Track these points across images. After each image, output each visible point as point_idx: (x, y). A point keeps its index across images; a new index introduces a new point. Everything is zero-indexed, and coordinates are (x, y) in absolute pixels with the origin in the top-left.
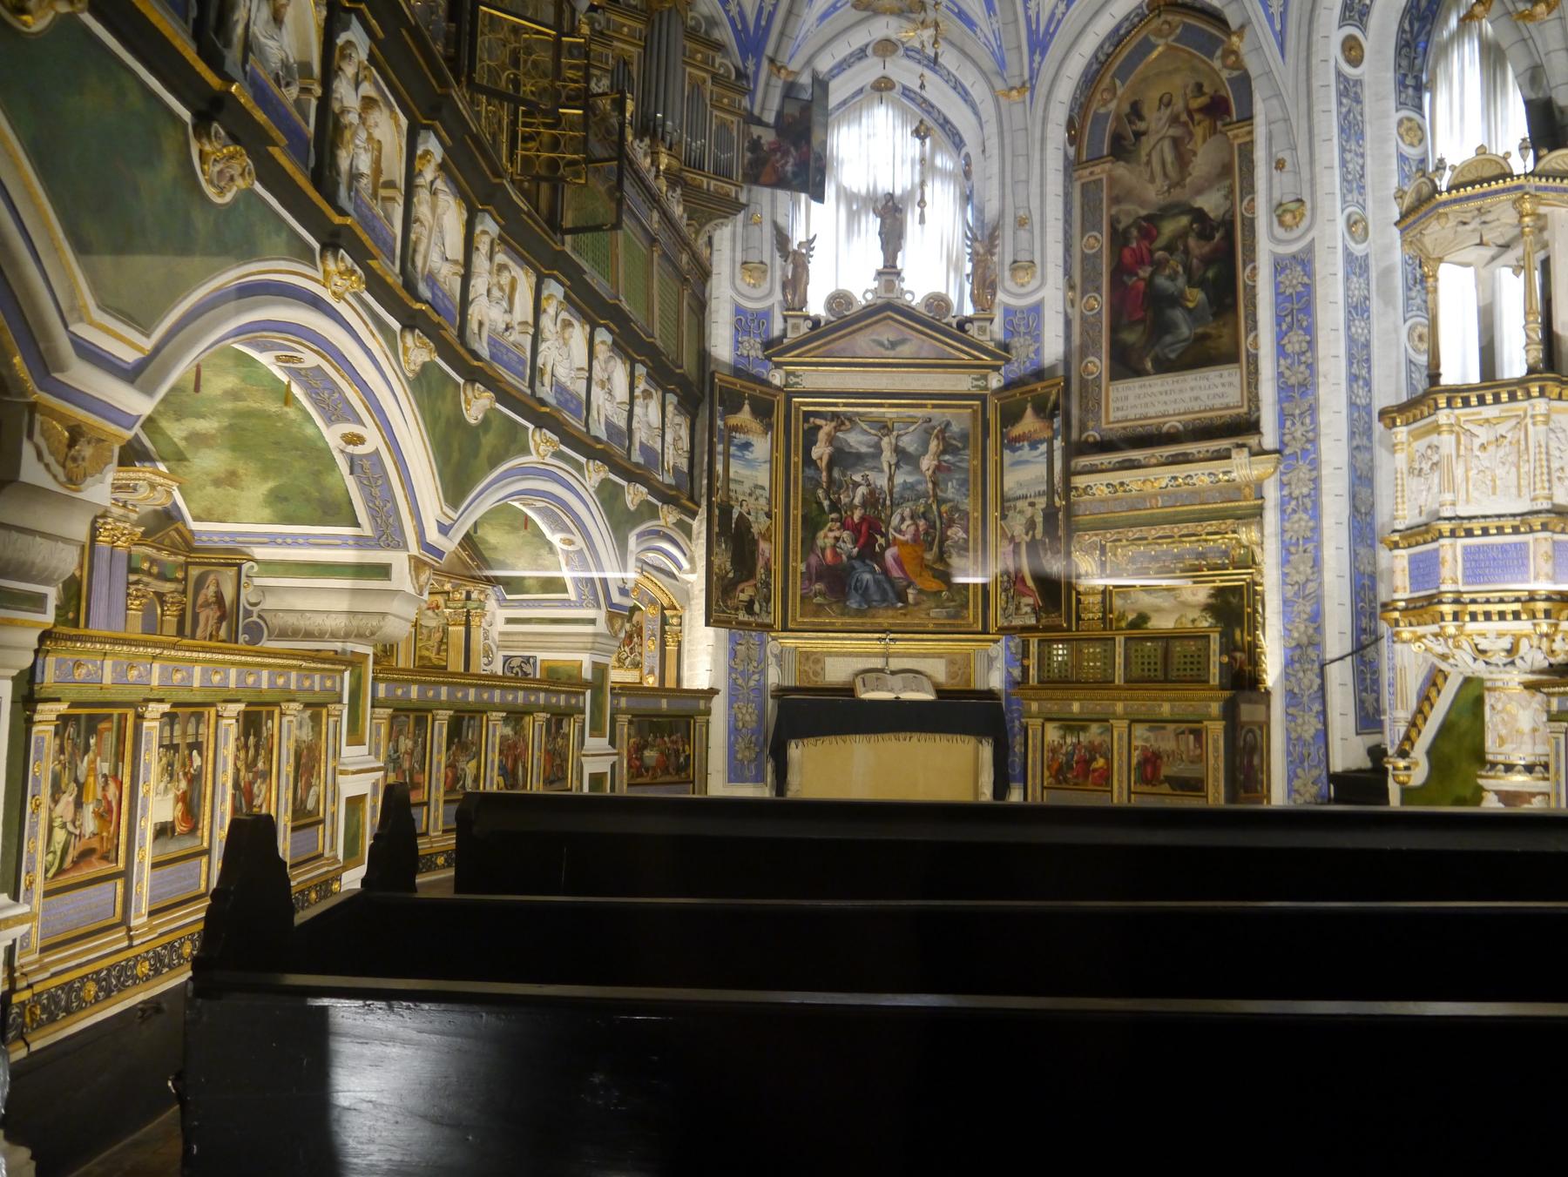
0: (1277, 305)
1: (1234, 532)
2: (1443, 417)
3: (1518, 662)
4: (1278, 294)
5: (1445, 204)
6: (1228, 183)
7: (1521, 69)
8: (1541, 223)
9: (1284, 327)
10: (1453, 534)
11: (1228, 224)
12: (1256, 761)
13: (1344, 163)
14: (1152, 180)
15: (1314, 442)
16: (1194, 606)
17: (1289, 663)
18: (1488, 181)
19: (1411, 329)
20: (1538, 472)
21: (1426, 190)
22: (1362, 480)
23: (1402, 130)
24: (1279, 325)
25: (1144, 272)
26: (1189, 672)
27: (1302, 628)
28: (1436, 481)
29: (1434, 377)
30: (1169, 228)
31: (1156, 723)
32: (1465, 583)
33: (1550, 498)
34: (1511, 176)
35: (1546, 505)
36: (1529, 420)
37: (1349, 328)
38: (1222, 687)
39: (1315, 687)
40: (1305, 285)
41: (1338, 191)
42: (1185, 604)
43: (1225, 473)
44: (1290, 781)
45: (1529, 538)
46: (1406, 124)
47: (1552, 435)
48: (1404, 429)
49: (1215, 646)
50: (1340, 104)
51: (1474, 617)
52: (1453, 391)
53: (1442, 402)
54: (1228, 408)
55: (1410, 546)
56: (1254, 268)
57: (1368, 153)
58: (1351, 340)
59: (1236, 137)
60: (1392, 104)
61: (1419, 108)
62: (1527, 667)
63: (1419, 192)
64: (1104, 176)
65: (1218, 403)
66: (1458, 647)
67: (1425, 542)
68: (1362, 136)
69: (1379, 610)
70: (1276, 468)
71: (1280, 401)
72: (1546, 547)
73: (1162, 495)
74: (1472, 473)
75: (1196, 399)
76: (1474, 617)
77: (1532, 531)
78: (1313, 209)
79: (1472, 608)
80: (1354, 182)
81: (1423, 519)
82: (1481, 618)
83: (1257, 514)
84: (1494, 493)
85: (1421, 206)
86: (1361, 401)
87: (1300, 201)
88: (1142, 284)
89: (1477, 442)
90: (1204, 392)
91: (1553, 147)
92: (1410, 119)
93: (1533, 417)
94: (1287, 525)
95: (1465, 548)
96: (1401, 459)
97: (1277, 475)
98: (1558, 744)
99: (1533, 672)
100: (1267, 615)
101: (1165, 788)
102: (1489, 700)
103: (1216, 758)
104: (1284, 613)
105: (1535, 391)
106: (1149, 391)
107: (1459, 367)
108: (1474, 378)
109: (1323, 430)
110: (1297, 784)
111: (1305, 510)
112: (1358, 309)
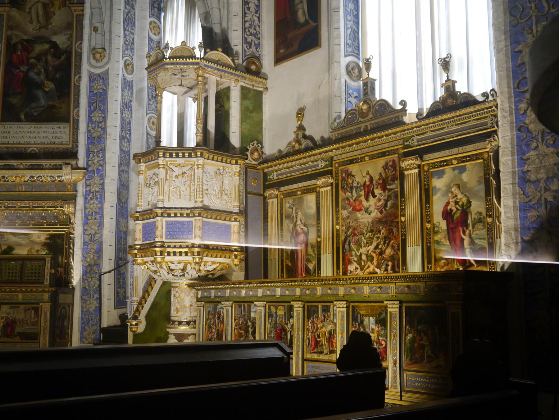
0: (90, 97)
1: (61, 207)
2: (161, 161)
3: (186, 275)
4: (90, 92)
5: (168, 64)
6: (70, 32)
7: (201, 12)
8: (205, 81)
9: (92, 108)
10: (162, 215)
11: (68, 52)
12: (66, 323)
13: (125, 36)
14: (31, 22)
15: (103, 166)
16: (38, 244)
17: (84, 274)
18: (186, 57)
19: (149, 119)
20: (198, 190)
21: (160, 56)
22: (123, 186)
23: (151, 27)
24: (90, 107)
25: (24, 68)
26: (33, 278)
27: (92, 256)
28: (156, 190)
29: (158, 142)
30: (39, 48)
31: (14, 305)
32: (166, 238)
33: (202, 202)
34: (195, 57)
35: (200, 205)
36: (196, 167)
37: (122, 114)
38: (51, 286)
39: (96, 286)
40: (103, 90)
41: (121, 48)
42: (34, 242)
43: (59, 177)
44: (82, 333)
45: (193, 219)
46: (153, 24)
47: (204, 175)
48: (144, 164)
49: (48, 265)
50: (125, 8)
52: (166, 149)
53: (161, 154)
54: (62, 144)
55: (143, 220)
56: (80, 77)
57: (136, 33)
58: (123, 119)
59: (75, 11)
60: (148, 13)
61: (159, 19)
62: (189, 277)
63: (157, 56)
64: (5, 14)
65: (57, 141)
66: (161, 268)
67: (150, 218)
68: (134, 25)
69: (128, 250)
70: (84, 177)
71: (88, 144)
72: (199, 224)
73: (25, 185)
75: (46, 137)
77: (194, 216)
78: (110, 54)
79: (168, 250)
80: (129, 46)
81: (150, 207)
82: (172, 254)
83: (72, 199)
85: (157, 63)
86: (126, 149)
87: (104, 49)
88: (22, 74)
90: (51, 134)
91: (213, 48)
92: (155, 23)
93: (197, 165)
94: (88, 205)
95: (167, 222)
96: (142, 177)
98: (200, 312)
99: (192, 280)
101: (18, 339)
102: (173, 293)
103: (45, 322)
104: (83, 248)
105: (199, 154)
106: (22, 130)
107: (169, 139)
108: (175, 145)
109: (107, 161)
110: (85, 333)
111: (97, 199)
112: (126, 106)
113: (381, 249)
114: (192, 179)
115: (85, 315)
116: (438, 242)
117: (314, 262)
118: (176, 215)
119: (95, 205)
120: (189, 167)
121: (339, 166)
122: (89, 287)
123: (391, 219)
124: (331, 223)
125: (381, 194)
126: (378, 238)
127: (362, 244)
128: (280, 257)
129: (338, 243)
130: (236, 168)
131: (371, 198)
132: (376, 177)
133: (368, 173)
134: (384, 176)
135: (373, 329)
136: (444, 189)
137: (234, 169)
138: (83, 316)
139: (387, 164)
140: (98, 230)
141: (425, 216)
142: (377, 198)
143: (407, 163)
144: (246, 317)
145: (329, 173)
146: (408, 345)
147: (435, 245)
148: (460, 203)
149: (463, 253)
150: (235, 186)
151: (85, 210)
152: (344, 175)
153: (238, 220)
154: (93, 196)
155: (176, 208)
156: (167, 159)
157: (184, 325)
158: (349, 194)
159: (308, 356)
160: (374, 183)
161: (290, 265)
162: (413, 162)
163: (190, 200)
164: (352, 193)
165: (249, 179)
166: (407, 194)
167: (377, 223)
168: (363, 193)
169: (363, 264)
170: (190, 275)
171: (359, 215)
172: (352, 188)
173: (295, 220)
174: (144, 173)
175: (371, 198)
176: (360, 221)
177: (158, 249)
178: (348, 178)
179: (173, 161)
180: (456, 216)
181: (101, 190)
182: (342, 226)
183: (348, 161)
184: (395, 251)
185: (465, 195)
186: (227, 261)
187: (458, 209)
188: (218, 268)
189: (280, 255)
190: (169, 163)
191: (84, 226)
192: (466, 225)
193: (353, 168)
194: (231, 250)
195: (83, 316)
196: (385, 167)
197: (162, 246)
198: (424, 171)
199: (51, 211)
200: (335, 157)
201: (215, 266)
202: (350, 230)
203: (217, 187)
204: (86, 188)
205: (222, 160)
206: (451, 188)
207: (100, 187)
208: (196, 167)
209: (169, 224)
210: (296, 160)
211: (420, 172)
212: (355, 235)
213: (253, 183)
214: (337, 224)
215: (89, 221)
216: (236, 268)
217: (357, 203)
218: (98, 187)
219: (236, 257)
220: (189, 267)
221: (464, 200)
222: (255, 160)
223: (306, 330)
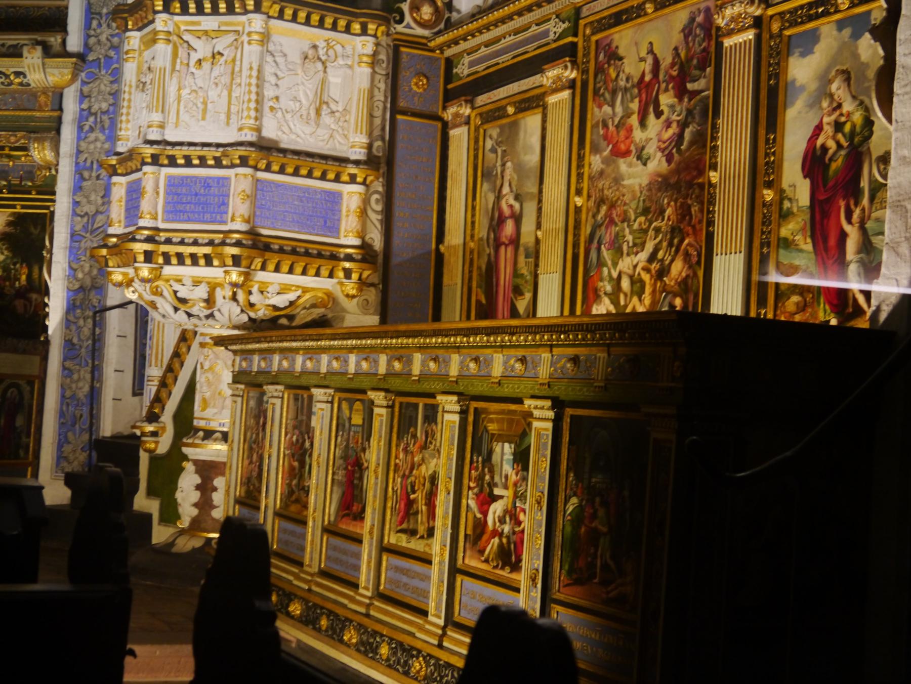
3: (216, 314)
10: (155, 160)
12: (20, 421)
17: (71, 308)
20: (246, 98)
27: (87, 269)
32: (164, 221)
33: (259, 130)
35: (250, 137)
36: (245, 38)
43: (18, 74)
44: (60, 446)
45: (230, 173)
47: (269, 59)
51: (167, 261)
74: (185, 92)
76: (181, 258)
77: (233, 166)
84: (203, 119)
89: (195, 57)
93: (249, 34)
94: (83, 145)
95: (170, 179)
97: (78, 84)
99: (235, 327)
100: (54, 251)
104: (71, 248)
110: (67, 448)
111: (103, 129)
113: (662, 260)
114: (237, 69)
115: (68, 404)
116: (786, 244)
117: (528, 296)
118: (188, 163)
119: (99, 144)
120: (231, 38)
121: (593, 34)
122: (80, 340)
123: (688, 178)
124: (564, 188)
125: (672, 107)
126: (657, 230)
127: (625, 247)
128: (466, 281)
129: (576, 245)
130: (364, 45)
131: (652, 117)
132: (666, 60)
133: (651, 51)
134: (683, 55)
135: (506, 477)
136: (813, 86)
137: (359, 46)
138: (64, 408)
139: (692, 20)
140: (103, 204)
141: (763, 169)
142: (664, 117)
143: (729, 12)
144: (304, 429)
145: (570, 51)
146: (568, 529)
147: (781, 251)
148: (847, 128)
149: (843, 276)
150: (360, 90)
151: (77, 158)
152: (602, 56)
153: (359, 179)
154: (95, 122)
155: (191, 144)
156: (176, 18)
157: (215, 440)
158: (607, 109)
159: (393, 539)
160: (661, 77)
161: (484, 301)
162: (742, 10)
163: (228, 124)
164: (613, 106)
165: (404, 74)
166: (724, 101)
167: (659, 190)
168: (635, 106)
169: (622, 303)
170: (227, 315)
171: (623, 165)
172: (614, 93)
173: (499, 183)
174: (136, 55)
175: (652, 117)
176: (625, 182)
177: (139, 247)
178: (609, 66)
179: (193, 23)
180: (834, 166)
181: (111, 108)
182: (589, 197)
183: (610, 16)
184: (690, 267)
185: (861, 103)
186: (323, 284)
187: (839, 146)
188: (301, 301)
189: (467, 276)
190: (183, 28)
191: (74, 194)
192: (854, 192)
193: (624, 38)
194: (334, 257)
195: (64, 408)
196: (687, 31)
197: (149, 240)
198: (772, 37)
199: (19, 157)
200: (585, 9)
201: (292, 296)
202: (604, 209)
203: (306, 91)
204: (81, 102)
205: (308, 18)
206: (830, 82)
207: (112, 101)
208: (245, 38)
209: (173, 185)
210: (503, 21)
211: (758, 37)
212: (612, 222)
213: (415, 86)
214: (579, 192)
215: (85, 184)
216: (351, 306)
217: (623, 133)
218: (106, 100)
219: (348, 273)
220: (219, 293)
221: (858, 117)
222: (422, 25)
223: (392, 468)
